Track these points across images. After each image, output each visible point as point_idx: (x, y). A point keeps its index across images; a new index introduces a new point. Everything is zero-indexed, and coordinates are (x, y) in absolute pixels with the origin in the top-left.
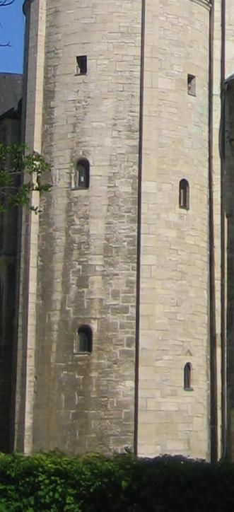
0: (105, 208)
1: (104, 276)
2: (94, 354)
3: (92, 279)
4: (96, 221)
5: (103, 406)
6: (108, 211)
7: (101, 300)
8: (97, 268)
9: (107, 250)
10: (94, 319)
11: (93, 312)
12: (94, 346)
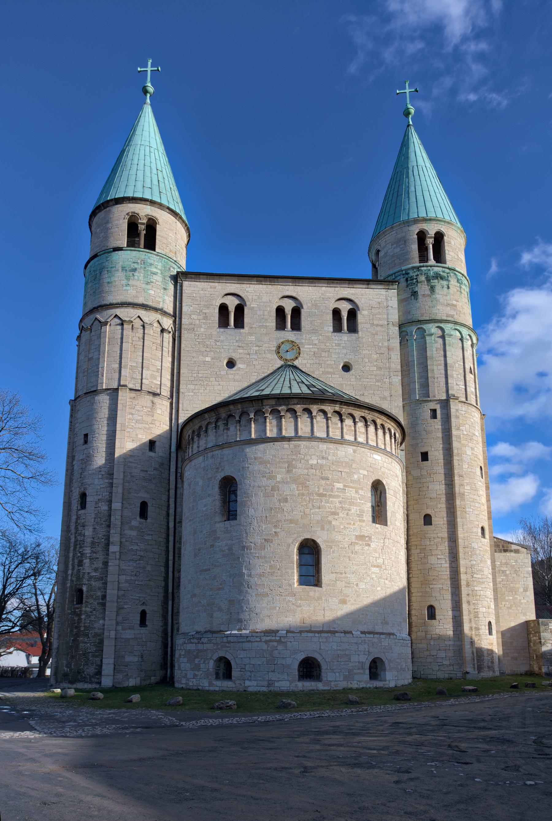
0: (93, 519)
1: (90, 559)
2: (84, 605)
3: (85, 561)
4: (88, 527)
5: (87, 635)
6: (94, 521)
7: (89, 573)
8: (88, 555)
9: (93, 543)
10: (85, 584)
11: (85, 580)
12: (84, 600)
